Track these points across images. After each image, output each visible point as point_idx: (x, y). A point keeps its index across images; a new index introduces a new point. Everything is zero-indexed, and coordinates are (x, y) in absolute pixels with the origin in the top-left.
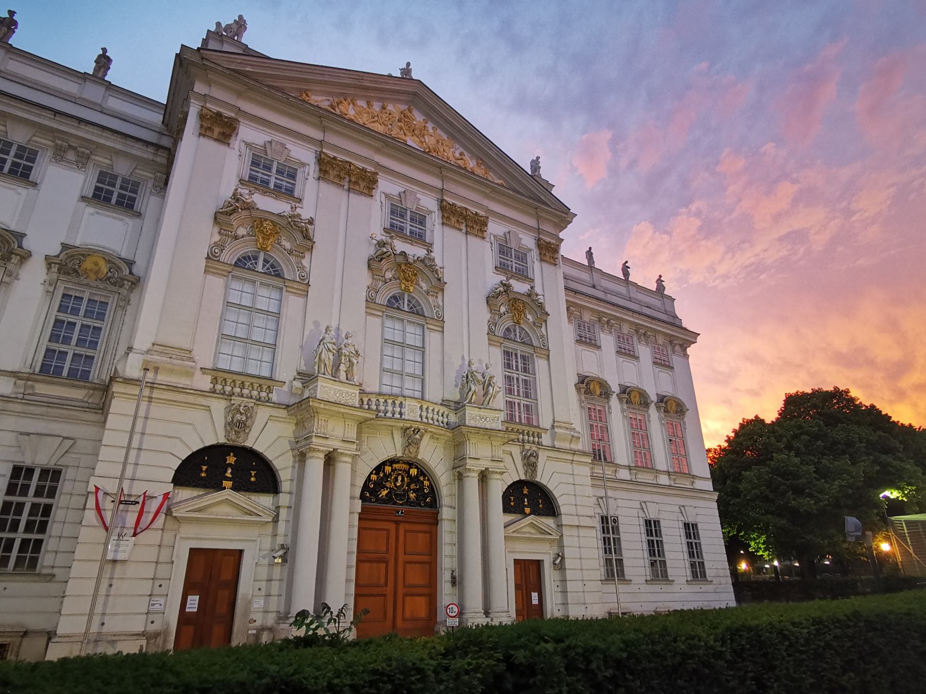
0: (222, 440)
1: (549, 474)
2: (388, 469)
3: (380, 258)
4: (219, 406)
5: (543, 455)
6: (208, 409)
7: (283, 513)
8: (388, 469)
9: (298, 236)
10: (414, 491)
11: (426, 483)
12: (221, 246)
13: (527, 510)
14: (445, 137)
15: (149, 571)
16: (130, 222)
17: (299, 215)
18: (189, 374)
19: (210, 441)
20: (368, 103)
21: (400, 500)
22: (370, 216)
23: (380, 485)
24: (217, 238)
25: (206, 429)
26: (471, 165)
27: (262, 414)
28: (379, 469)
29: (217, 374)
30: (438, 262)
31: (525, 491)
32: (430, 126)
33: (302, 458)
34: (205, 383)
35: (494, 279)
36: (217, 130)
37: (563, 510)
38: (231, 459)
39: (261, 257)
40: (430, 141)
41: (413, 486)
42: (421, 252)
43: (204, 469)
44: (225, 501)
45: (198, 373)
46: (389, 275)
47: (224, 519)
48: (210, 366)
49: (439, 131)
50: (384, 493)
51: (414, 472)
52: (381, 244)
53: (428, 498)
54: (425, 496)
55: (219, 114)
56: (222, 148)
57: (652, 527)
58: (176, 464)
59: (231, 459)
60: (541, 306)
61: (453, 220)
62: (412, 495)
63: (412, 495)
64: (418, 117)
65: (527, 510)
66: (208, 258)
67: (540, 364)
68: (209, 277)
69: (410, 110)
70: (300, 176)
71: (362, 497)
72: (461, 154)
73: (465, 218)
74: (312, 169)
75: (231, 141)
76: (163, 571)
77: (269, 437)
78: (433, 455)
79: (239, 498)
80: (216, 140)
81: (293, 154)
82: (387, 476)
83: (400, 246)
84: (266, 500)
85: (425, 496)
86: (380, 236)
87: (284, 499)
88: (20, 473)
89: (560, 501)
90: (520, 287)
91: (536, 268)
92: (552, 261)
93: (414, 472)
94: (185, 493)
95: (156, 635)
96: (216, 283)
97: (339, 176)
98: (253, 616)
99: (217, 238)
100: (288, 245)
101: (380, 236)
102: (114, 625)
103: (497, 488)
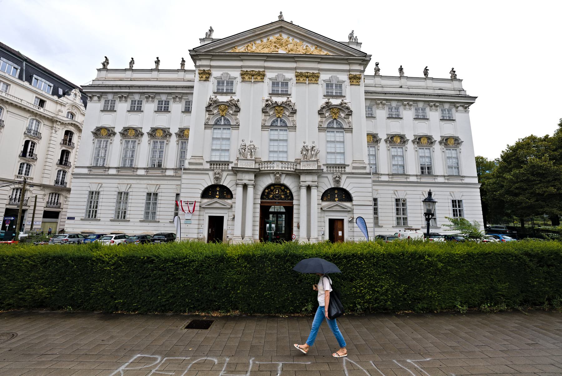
0: (213, 183)
2: (272, 188)
3: (267, 105)
4: (211, 173)
5: (344, 177)
6: (208, 174)
8: (272, 188)
9: (234, 108)
10: (283, 195)
12: (208, 119)
13: (337, 199)
14: (298, 41)
15: (197, 222)
17: (234, 100)
18: (201, 164)
19: (210, 184)
20: (262, 41)
22: (262, 91)
23: (269, 193)
25: (209, 181)
26: (312, 50)
27: (225, 174)
29: (211, 163)
30: (293, 101)
31: (336, 192)
32: (291, 38)
34: (208, 166)
35: (322, 102)
36: (204, 77)
37: (354, 198)
38: (218, 189)
39: (223, 118)
40: (290, 46)
42: (284, 99)
43: (208, 193)
44: (217, 202)
45: (205, 163)
46: (271, 113)
47: (217, 208)
48: (208, 160)
49: (296, 40)
51: (283, 188)
52: (267, 101)
55: (204, 71)
56: (207, 83)
58: (201, 192)
59: (218, 189)
60: (348, 108)
61: (301, 79)
62: (283, 196)
63: (283, 196)
64: (285, 37)
65: (337, 199)
66: (205, 124)
68: (206, 130)
69: (281, 36)
71: (262, 198)
72: (307, 46)
73: (307, 77)
74: (239, 79)
75: (209, 79)
76: (201, 222)
77: (227, 181)
79: (220, 201)
80: (205, 80)
82: (272, 191)
83: (275, 99)
86: (267, 97)
89: (353, 195)
90: (335, 102)
92: (357, 84)
95: (202, 239)
96: (209, 131)
98: (228, 235)
99: (207, 116)
100: (231, 112)
101: (267, 97)
102: (190, 236)
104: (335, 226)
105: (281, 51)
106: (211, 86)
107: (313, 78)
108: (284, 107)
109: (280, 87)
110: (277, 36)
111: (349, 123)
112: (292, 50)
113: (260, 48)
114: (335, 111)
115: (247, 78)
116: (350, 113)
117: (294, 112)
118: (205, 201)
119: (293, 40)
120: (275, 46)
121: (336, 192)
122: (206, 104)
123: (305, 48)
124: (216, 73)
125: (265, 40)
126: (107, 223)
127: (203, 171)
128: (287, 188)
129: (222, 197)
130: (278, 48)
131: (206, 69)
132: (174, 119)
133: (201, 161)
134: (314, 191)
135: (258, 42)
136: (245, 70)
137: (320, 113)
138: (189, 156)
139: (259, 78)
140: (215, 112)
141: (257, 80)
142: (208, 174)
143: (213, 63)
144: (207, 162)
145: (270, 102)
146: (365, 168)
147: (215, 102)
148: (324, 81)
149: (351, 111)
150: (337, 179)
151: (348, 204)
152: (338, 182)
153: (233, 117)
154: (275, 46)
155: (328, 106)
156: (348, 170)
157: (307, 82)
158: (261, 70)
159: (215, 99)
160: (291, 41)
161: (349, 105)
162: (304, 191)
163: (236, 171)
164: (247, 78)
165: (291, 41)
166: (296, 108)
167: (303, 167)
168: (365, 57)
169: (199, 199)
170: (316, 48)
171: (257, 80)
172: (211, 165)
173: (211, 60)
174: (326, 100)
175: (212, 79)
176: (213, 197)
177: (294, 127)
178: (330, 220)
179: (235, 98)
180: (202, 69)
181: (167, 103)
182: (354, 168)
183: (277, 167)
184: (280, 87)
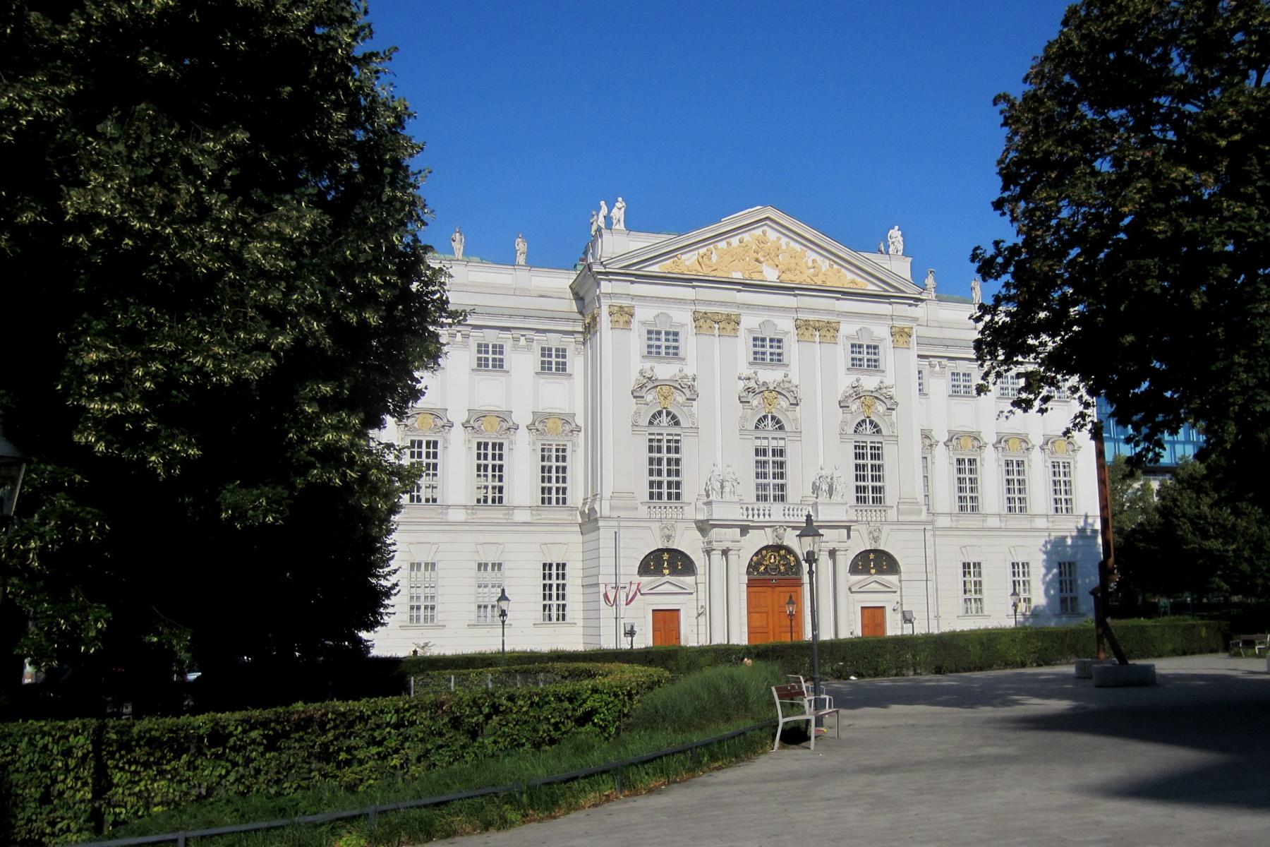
5: (886, 529)
7: (701, 587)
12: (637, 413)
13: (873, 571)
14: (798, 247)
16: (566, 382)
17: (686, 377)
21: (776, 574)
24: (635, 407)
27: (680, 526)
30: (795, 382)
31: (872, 556)
33: (708, 552)
34: (643, 511)
35: (845, 381)
44: (667, 582)
47: (666, 592)
49: (792, 244)
51: (783, 552)
64: (772, 235)
67: (888, 451)
69: (764, 233)
70: (681, 337)
71: (748, 573)
72: (814, 261)
77: (689, 542)
82: (763, 557)
84: (689, 580)
85: (791, 568)
87: (700, 578)
88: (547, 566)
90: (869, 382)
91: (888, 356)
94: (645, 579)
103: (844, 561)
106: (636, 340)
107: (827, 330)
109: (768, 350)
110: (758, 232)
111: (892, 424)
113: (727, 259)
114: (869, 401)
115: (705, 326)
119: (788, 244)
120: (757, 260)
121: (872, 556)
122: (632, 385)
123: (810, 264)
124: (644, 313)
125: (735, 241)
129: (674, 572)
131: (625, 302)
134: (840, 557)
135: (722, 245)
136: (702, 309)
137: (843, 406)
138: (607, 493)
139: (729, 327)
140: (649, 398)
141: (724, 333)
145: (752, 384)
148: (847, 337)
149: (897, 404)
150: (876, 534)
151: (891, 579)
152: (876, 539)
153: (685, 409)
155: (857, 393)
156: (892, 515)
157: (817, 339)
158: (732, 311)
160: (784, 247)
161: (893, 392)
164: (705, 326)
165: (784, 247)
166: (800, 395)
170: (831, 266)
174: (851, 379)
175: (635, 324)
176: (658, 572)
178: (863, 608)
179: (690, 370)
181: (499, 349)
184: (768, 350)
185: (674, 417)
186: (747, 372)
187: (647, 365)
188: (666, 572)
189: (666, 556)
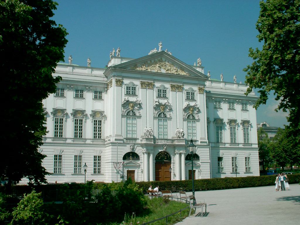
1: (199, 151)
4: (128, 146)
8: (160, 153)
11: (169, 156)
28: (158, 154)
29: (127, 139)
30: (170, 103)
35: (185, 104)
41: (166, 156)
50: (160, 158)
52: (156, 102)
53: (169, 158)
54: (169, 158)
57: (234, 159)
60: (198, 108)
66: (122, 115)
71: (155, 160)
78: (170, 151)
79: (133, 161)
81: (135, 84)
82: (160, 155)
85: (169, 158)
88: (95, 157)
93: (166, 153)
97: (145, 86)
99: (123, 109)
104: (191, 173)
105: (163, 71)
108: (165, 106)
109: (162, 94)
112: (168, 70)
116: (199, 111)
117: (171, 110)
118: (126, 162)
126: (69, 176)
127: (124, 144)
128: (167, 153)
130: (160, 68)
132: (88, 103)
133: (122, 138)
142: (126, 146)
143: (124, 74)
144: (125, 138)
145: (157, 103)
146: (206, 142)
147: (128, 101)
154: (159, 66)
159: (127, 99)
162: (177, 156)
163: (142, 145)
167: (176, 143)
168: (207, 78)
169: (122, 161)
171: (149, 88)
172: (126, 140)
173: (122, 72)
177: (170, 119)
180: (118, 78)
182: (201, 142)
183: (163, 142)
185: (134, 113)
186: (157, 100)
187: (126, 98)
188: (131, 159)
189: (131, 154)
